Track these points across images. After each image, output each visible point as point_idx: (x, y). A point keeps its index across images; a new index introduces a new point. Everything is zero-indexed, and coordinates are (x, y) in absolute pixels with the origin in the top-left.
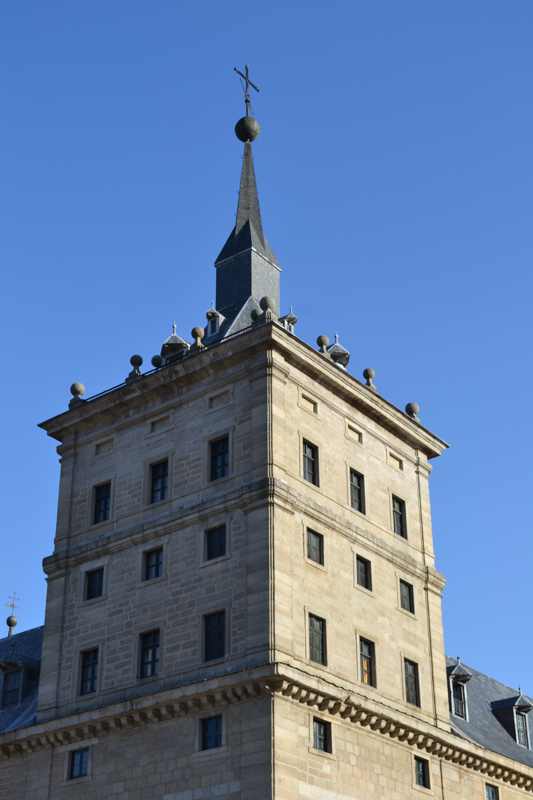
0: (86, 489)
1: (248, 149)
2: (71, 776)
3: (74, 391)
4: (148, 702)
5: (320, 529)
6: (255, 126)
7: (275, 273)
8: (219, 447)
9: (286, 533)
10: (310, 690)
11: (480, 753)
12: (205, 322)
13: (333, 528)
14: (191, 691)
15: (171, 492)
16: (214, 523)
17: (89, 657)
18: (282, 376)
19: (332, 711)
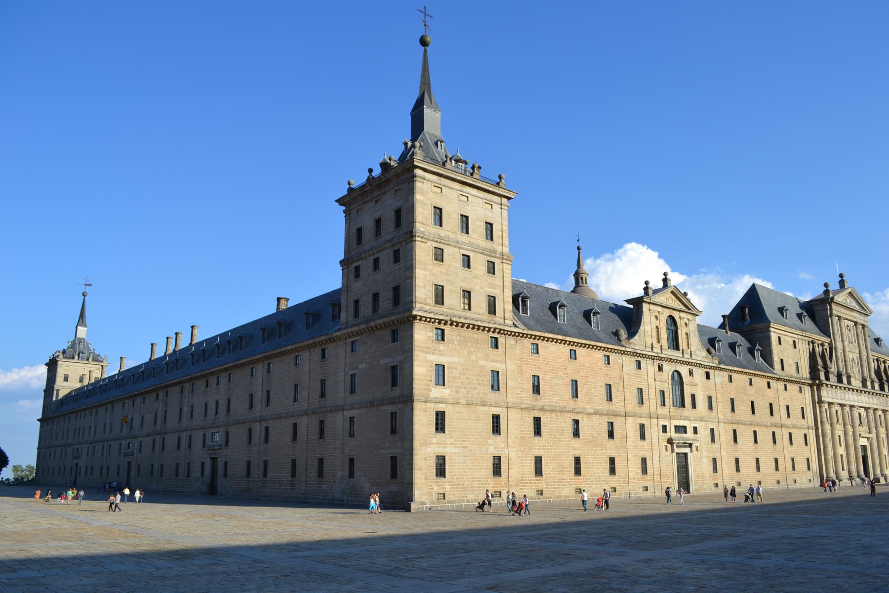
0: (354, 230)
1: (425, 51)
2: (352, 351)
3: (349, 183)
4: (373, 324)
5: (442, 246)
6: (428, 39)
7: (438, 115)
8: (398, 212)
9: (422, 252)
10: (431, 318)
11: (525, 332)
12: (403, 148)
14: (386, 320)
15: (382, 232)
16: (396, 248)
17: (357, 302)
18: (421, 180)
19: (445, 324)
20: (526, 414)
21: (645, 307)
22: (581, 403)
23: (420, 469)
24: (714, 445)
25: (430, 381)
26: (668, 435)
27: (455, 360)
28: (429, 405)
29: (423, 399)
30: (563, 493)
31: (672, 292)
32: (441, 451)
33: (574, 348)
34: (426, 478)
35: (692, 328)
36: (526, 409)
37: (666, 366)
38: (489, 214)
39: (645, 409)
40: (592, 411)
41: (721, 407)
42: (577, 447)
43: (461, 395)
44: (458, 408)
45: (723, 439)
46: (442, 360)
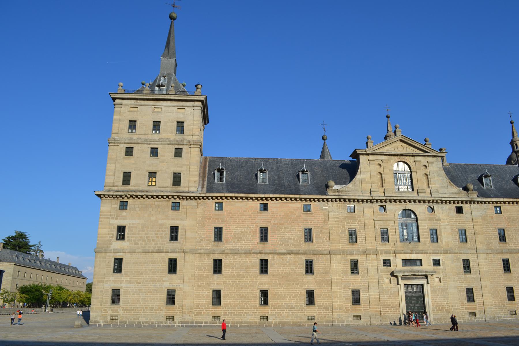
5: (132, 146)
13: (139, 143)
18: (120, 106)
20: (205, 257)
21: (362, 159)
22: (269, 246)
23: (97, 298)
24: (468, 276)
25: (112, 237)
26: (392, 268)
27: (136, 221)
28: (108, 254)
29: (103, 250)
30: (244, 320)
31: (401, 140)
32: (117, 286)
33: (265, 202)
34: (101, 305)
35: (435, 167)
36: (205, 253)
37: (389, 206)
38: (182, 116)
39: (359, 246)
40: (285, 251)
41: (483, 238)
42: (265, 282)
43: (139, 246)
44: (134, 255)
45: (485, 268)
46: (121, 223)
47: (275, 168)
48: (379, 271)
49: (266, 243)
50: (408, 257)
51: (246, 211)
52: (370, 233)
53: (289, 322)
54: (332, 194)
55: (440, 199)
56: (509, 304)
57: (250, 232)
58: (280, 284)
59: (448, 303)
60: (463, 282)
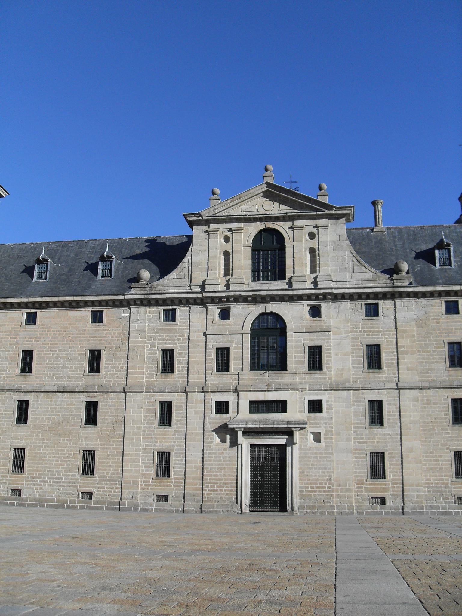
22: (33, 379)
24: (377, 430)
37: (235, 309)
40: (56, 388)
42: (21, 436)
47: (72, 255)
48: (207, 421)
49: (28, 374)
50: (260, 396)
51: (5, 325)
52: (197, 356)
53: (52, 500)
54: (139, 292)
55: (329, 291)
56: (458, 484)
57: (7, 358)
58: (44, 439)
59: (330, 480)
60: (365, 442)
